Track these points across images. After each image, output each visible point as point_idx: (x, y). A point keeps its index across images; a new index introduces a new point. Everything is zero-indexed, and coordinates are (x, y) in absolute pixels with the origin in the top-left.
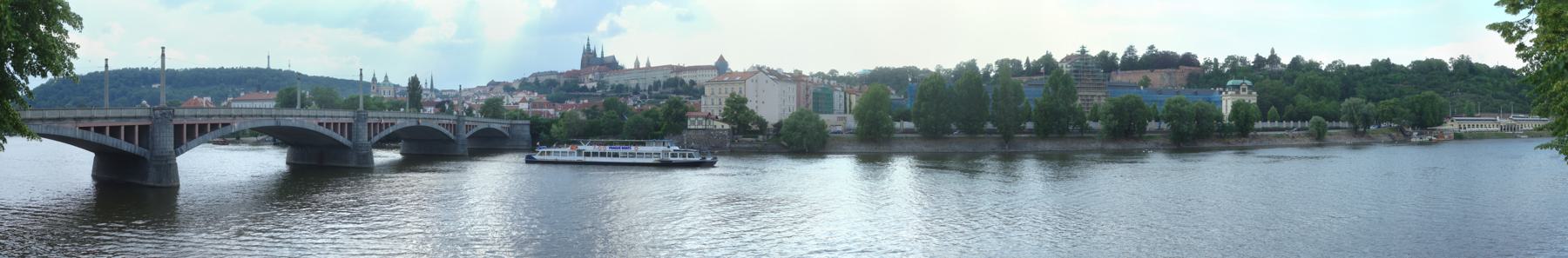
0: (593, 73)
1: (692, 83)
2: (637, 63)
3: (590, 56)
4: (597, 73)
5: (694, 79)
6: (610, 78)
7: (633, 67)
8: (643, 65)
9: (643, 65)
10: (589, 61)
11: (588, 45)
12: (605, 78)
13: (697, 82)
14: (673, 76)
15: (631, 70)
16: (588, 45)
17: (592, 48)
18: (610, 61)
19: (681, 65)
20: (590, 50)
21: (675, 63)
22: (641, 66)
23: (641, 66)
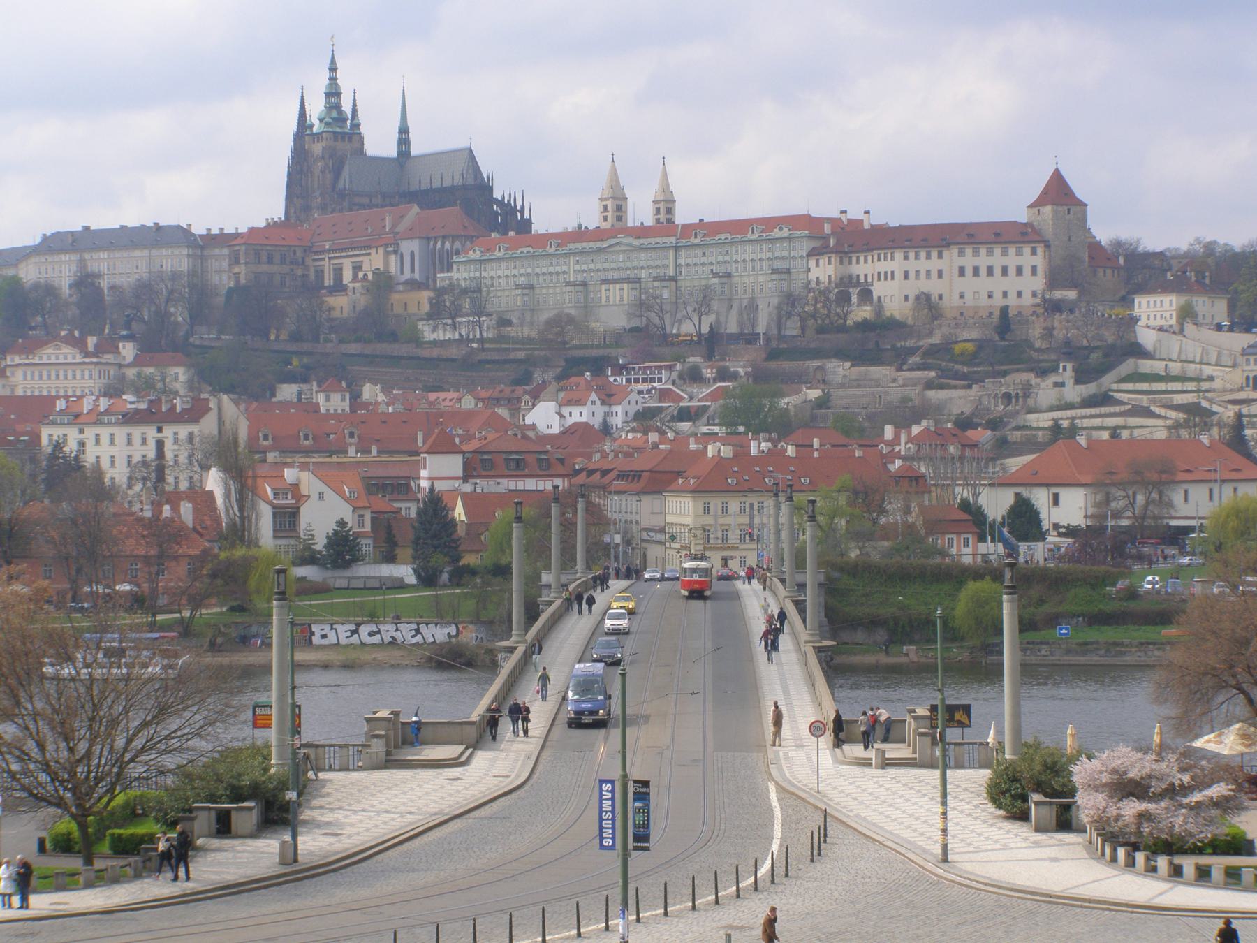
0: (392, 245)
1: (926, 303)
2: (617, 203)
3: (340, 146)
4: (410, 246)
5: (933, 287)
6: (489, 272)
7: (592, 220)
8: (641, 212)
9: (641, 212)
10: (337, 172)
11: (333, 93)
12: (460, 275)
13: (951, 302)
14: (823, 271)
15: (580, 234)
16: (333, 93)
17: (347, 107)
18: (454, 176)
19: (855, 213)
20: (341, 119)
21: (825, 207)
22: (632, 221)
23: (632, 221)
